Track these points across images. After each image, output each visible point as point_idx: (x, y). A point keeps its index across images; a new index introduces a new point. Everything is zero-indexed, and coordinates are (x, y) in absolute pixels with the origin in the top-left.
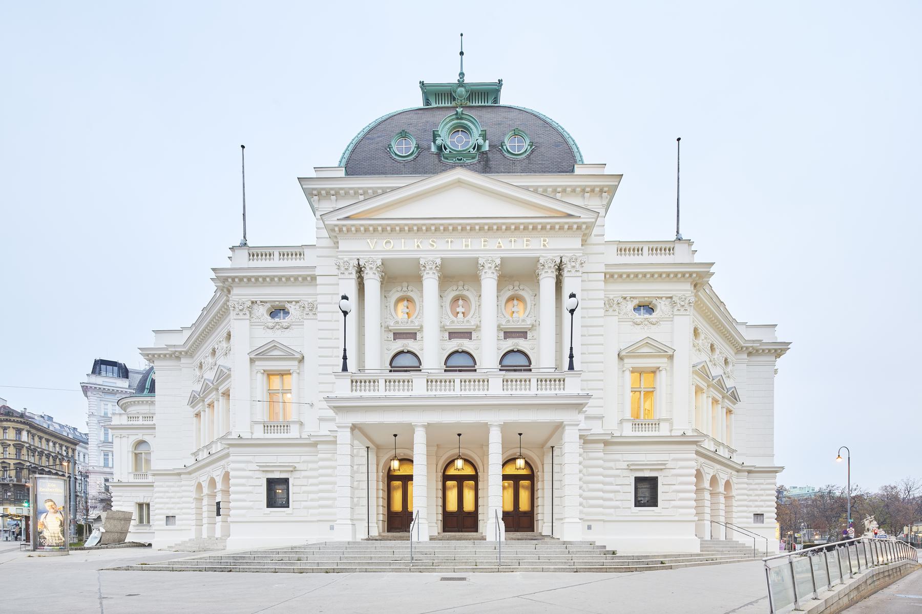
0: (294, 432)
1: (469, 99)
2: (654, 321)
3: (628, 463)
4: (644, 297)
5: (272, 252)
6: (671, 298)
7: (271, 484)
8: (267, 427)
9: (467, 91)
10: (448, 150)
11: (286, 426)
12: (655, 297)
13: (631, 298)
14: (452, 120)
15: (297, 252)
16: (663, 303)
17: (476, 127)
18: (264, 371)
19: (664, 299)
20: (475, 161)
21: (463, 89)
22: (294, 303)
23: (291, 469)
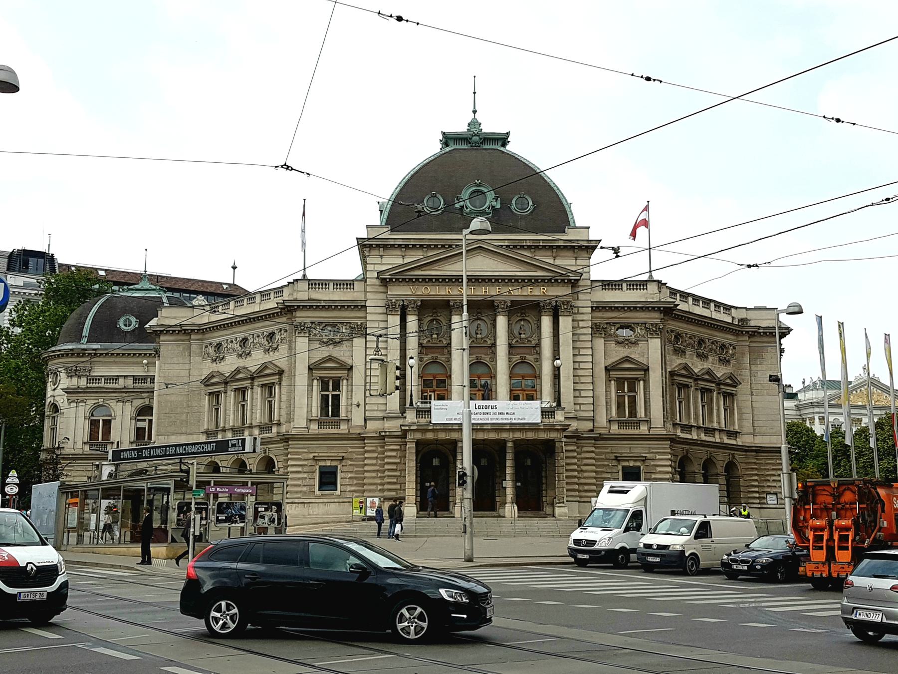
0: (344, 427)
1: (482, 143)
2: (633, 342)
3: (616, 455)
5: (327, 283)
6: (646, 324)
8: (320, 423)
9: (481, 139)
10: (469, 210)
11: (337, 425)
13: (613, 323)
16: (639, 328)
19: (640, 325)
21: (477, 138)
22: (345, 324)
23: (341, 458)
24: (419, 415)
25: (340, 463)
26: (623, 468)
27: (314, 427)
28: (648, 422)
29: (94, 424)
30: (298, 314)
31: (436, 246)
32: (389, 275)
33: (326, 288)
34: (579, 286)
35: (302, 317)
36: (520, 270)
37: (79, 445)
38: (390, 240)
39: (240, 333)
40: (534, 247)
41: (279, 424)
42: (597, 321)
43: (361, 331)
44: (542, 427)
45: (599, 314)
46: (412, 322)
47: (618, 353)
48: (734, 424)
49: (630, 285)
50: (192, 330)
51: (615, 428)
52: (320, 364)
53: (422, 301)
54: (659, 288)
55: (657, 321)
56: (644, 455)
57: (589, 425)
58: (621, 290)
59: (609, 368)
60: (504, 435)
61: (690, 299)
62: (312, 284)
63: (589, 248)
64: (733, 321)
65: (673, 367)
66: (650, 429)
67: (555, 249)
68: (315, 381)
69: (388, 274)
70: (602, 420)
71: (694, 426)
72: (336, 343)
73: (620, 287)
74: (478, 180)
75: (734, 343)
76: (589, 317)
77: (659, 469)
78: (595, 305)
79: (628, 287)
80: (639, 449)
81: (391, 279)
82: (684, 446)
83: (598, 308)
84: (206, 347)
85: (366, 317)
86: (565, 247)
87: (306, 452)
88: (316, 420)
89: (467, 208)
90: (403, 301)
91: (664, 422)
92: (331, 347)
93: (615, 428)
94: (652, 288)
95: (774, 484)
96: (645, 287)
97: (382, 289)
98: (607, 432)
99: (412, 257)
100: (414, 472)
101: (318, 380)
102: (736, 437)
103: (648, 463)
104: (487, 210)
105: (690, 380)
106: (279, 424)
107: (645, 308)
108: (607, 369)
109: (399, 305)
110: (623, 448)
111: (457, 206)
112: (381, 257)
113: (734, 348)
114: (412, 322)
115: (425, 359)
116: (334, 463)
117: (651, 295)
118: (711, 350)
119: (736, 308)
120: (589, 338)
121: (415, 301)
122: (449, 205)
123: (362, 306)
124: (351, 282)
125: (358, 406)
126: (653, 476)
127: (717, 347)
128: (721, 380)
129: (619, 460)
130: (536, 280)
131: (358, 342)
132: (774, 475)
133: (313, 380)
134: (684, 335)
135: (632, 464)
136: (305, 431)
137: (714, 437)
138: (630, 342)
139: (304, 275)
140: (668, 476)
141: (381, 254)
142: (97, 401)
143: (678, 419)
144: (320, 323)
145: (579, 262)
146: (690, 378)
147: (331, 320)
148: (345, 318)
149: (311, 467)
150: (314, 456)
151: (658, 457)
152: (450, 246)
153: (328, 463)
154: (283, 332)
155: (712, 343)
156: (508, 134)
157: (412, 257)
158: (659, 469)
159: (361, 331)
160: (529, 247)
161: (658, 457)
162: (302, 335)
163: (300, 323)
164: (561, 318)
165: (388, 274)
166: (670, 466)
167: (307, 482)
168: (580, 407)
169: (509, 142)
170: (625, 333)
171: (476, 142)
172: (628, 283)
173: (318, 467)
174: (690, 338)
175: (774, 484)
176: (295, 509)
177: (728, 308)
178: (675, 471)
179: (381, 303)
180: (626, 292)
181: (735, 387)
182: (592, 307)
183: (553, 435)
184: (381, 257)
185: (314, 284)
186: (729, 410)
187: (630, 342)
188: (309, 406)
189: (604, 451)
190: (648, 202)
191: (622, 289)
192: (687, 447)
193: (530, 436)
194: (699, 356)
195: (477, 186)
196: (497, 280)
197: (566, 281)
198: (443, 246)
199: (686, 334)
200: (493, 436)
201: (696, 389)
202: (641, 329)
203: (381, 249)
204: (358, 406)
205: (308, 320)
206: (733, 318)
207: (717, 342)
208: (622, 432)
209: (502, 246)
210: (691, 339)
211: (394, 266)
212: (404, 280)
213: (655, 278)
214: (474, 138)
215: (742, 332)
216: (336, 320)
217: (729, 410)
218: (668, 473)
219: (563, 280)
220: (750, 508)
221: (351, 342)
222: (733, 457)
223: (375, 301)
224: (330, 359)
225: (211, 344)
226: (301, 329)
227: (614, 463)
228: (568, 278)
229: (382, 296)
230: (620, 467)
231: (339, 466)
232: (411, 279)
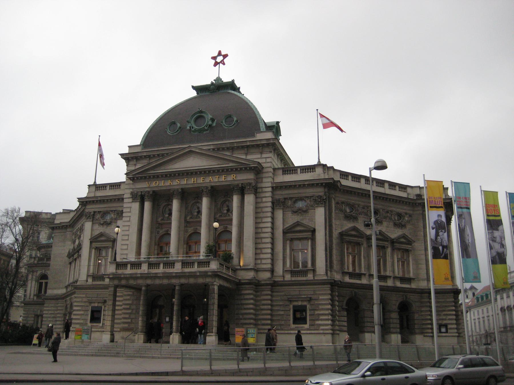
4: (298, 197)
6: (313, 196)
7: (93, 312)
13: (290, 198)
14: (198, 114)
15: (117, 185)
18: (96, 247)
19: (310, 197)
20: (208, 132)
22: (114, 211)
23: (103, 301)
24: (119, 267)
25: (103, 305)
26: (294, 306)
27: (90, 280)
28: (314, 271)
29: (41, 284)
32: (132, 175)
34: (263, 173)
36: (216, 164)
37: (32, 297)
40: (232, 148)
42: (277, 197)
45: (279, 192)
46: (147, 205)
47: (292, 219)
48: (409, 272)
49: (303, 170)
50: (67, 226)
51: (288, 277)
52: (96, 238)
54: (324, 170)
55: (322, 194)
56: (309, 296)
57: (268, 275)
58: (296, 174)
59: (285, 231)
60: (174, 281)
61: (363, 181)
62: (98, 188)
64: (408, 196)
65: (344, 229)
66: (314, 277)
67: (248, 148)
68: (93, 251)
69: (131, 175)
70: (279, 269)
71: (365, 274)
73: (296, 171)
75: (411, 212)
76: (270, 194)
77: (321, 307)
78: (275, 186)
79: (302, 171)
80: (307, 291)
82: (351, 289)
83: (276, 188)
85: (123, 206)
86: (253, 146)
87: (84, 297)
89: (193, 128)
91: (326, 270)
92: (105, 226)
93: (288, 277)
94: (319, 170)
95: (444, 317)
96: (314, 170)
98: (282, 279)
100: (111, 309)
101: (95, 249)
102: (411, 282)
103: (312, 302)
104: (206, 127)
105: (360, 239)
107: (311, 184)
108: (285, 232)
110: (294, 291)
112: (135, 165)
113: (410, 216)
114: (147, 205)
115: (161, 232)
116: (100, 305)
117: (319, 174)
118: (385, 218)
119: (412, 187)
120: (270, 209)
121: (149, 192)
126: (316, 312)
127: (392, 215)
128: (393, 239)
129: (291, 301)
130: (227, 170)
132: (444, 311)
133: (93, 248)
134: (357, 206)
135: (300, 303)
136: (84, 283)
137: (386, 282)
139: (95, 182)
140: (327, 312)
141: (135, 163)
142: (41, 271)
143: (346, 269)
144: (99, 212)
145: (264, 156)
146: (362, 238)
147: (105, 209)
150: (88, 300)
151: (321, 297)
153: (96, 305)
155: (387, 212)
156: (233, 81)
158: (321, 307)
161: (321, 297)
162: (87, 220)
163: (88, 212)
164: (246, 197)
165: (131, 175)
166: (330, 304)
167: (83, 317)
168: (261, 261)
169: (239, 88)
170: (300, 204)
172: (302, 168)
173: (90, 307)
174: (363, 208)
175: (444, 317)
177: (403, 188)
178: (343, 308)
180: (300, 174)
181: (411, 245)
182: (272, 187)
183: (208, 280)
185: (103, 186)
186: (404, 263)
188: (89, 266)
189: (280, 294)
191: (297, 173)
192: (356, 290)
193: (192, 281)
194: (348, 217)
196: (201, 172)
197: (248, 168)
199: (359, 205)
200: (165, 281)
201: (369, 246)
202: (310, 201)
205: (92, 211)
206: (408, 194)
207: (391, 211)
208: (293, 279)
209: (209, 149)
210: (364, 209)
213: (323, 162)
214: (211, 87)
215: (416, 204)
216: (109, 209)
217: (404, 263)
218: (328, 309)
219: (246, 168)
220: (425, 336)
222: (406, 297)
224: (101, 235)
227: (287, 303)
228: (248, 166)
230: (291, 306)
231: (103, 307)
232: (145, 177)
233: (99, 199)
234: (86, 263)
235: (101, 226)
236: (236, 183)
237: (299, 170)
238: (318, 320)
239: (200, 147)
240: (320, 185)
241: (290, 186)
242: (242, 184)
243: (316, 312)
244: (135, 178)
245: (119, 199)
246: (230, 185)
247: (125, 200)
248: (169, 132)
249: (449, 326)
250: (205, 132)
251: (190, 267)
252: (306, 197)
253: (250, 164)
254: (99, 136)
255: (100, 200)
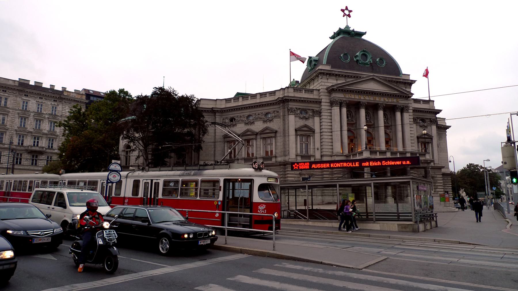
6: (430, 119)
8: (302, 157)
9: (355, 33)
10: (361, 62)
12: (426, 118)
13: (419, 118)
17: (369, 55)
22: (310, 110)
27: (299, 159)
30: (290, 103)
31: (351, 76)
32: (336, 87)
33: (301, 92)
35: (292, 105)
36: (388, 90)
38: (333, 72)
39: (247, 113)
41: (276, 157)
43: (319, 113)
44: (423, 161)
46: (344, 110)
50: (218, 111)
52: (301, 128)
53: (349, 101)
58: (420, 104)
63: (411, 83)
66: (434, 164)
69: (336, 87)
72: (307, 119)
74: (365, 49)
77: (439, 181)
81: (336, 89)
83: (415, 110)
84: (224, 119)
86: (402, 82)
88: (300, 155)
89: (360, 61)
90: (341, 100)
92: (304, 120)
95: (447, 188)
97: (327, 94)
99: (341, 81)
106: (276, 157)
109: (339, 102)
111: (355, 60)
112: (328, 79)
121: (346, 101)
122: (352, 59)
123: (319, 102)
124: (312, 90)
125: (318, 149)
126: (437, 184)
131: (317, 119)
132: (447, 184)
138: (425, 127)
141: (327, 78)
147: (304, 108)
148: (310, 107)
149: (298, 178)
152: (357, 77)
154: (276, 112)
157: (341, 81)
158: (439, 181)
159: (319, 113)
160: (389, 81)
163: (291, 108)
165: (336, 87)
171: (352, 34)
173: (301, 178)
175: (447, 188)
176: (292, 198)
179: (328, 101)
184: (328, 79)
187: (425, 127)
188: (296, 148)
190: (427, 67)
191: (420, 103)
195: (364, 52)
198: (354, 77)
203: (328, 76)
204: (318, 149)
211: (334, 84)
212: (342, 90)
221: (313, 119)
223: (325, 99)
225: (227, 118)
226: (291, 111)
229: (328, 97)
233: (302, 99)
234: (294, 146)
235: (301, 119)
236: (400, 105)
237: (421, 102)
238: (437, 189)
239: (381, 77)
240: (435, 113)
241: (421, 111)
242: (403, 106)
243: (437, 184)
244: (338, 90)
245: (316, 102)
246: (396, 105)
247: (323, 104)
248: (343, 60)
249: (449, 192)
250: (367, 66)
251: (372, 155)
252: (427, 118)
253: (409, 95)
254: (290, 49)
255: (302, 100)
